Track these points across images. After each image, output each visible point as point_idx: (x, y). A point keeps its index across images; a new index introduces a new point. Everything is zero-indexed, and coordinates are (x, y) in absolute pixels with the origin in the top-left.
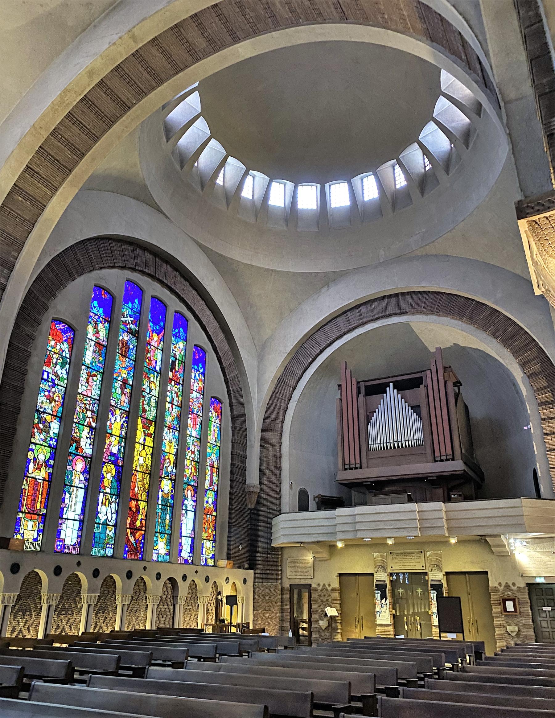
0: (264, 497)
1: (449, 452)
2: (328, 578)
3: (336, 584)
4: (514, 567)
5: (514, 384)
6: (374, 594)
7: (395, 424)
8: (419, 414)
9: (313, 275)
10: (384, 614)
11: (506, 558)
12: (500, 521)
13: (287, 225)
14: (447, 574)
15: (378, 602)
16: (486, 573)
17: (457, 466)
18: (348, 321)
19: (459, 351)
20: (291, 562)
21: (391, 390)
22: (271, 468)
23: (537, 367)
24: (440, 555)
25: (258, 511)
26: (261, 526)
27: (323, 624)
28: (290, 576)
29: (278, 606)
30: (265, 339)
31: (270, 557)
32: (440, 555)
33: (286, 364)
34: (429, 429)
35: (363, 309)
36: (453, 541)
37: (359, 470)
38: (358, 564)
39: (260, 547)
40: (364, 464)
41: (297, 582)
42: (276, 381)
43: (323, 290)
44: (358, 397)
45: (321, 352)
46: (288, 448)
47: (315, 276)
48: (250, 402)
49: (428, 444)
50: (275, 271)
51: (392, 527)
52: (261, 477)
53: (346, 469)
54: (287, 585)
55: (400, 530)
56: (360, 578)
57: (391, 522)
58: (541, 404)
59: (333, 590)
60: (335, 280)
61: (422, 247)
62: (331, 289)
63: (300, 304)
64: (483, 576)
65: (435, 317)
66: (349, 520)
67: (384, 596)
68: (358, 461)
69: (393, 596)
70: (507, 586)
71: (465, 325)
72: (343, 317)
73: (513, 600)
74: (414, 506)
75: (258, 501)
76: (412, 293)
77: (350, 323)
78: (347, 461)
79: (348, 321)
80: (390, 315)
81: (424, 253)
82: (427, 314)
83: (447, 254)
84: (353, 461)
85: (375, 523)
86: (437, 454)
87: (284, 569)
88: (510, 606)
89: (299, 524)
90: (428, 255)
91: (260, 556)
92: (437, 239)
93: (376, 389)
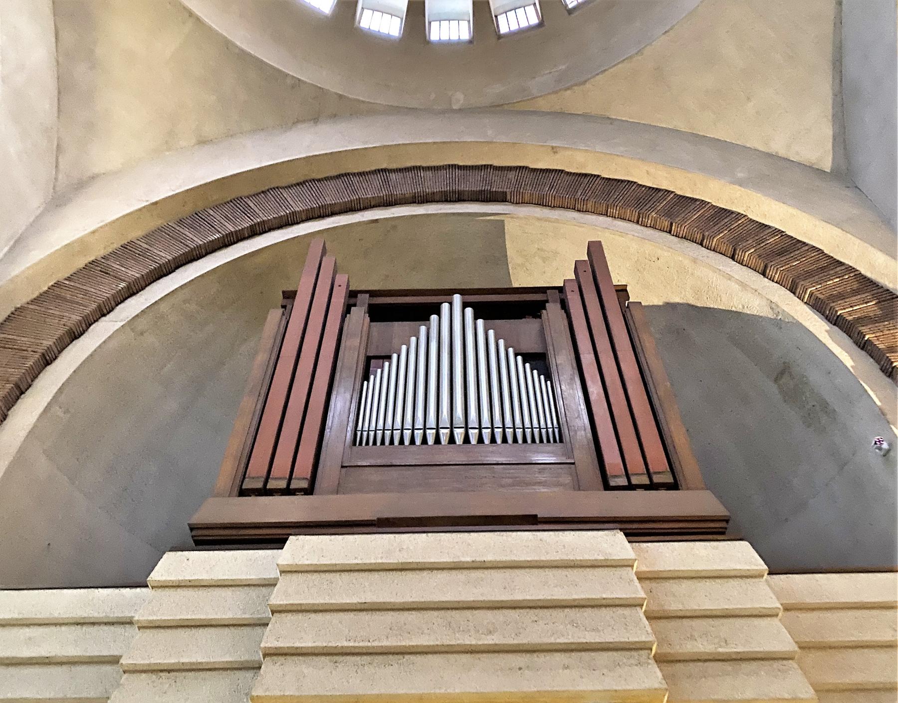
9: (289, 81)
30: (96, 170)
33: (135, 234)
35: (393, 176)
37: (299, 499)
42: (81, 262)
44: (347, 310)
45: (254, 232)
46: (23, 434)
47: (293, 87)
51: (489, 640)
53: (243, 493)
55: (541, 659)
57: (489, 615)
60: (335, 116)
61: (556, 92)
63: (230, 135)
78: (258, 466)
81: (557, 108)
83: (607, 114)
85: (390, 617)
90: (564, 113)
92: (594, 77)
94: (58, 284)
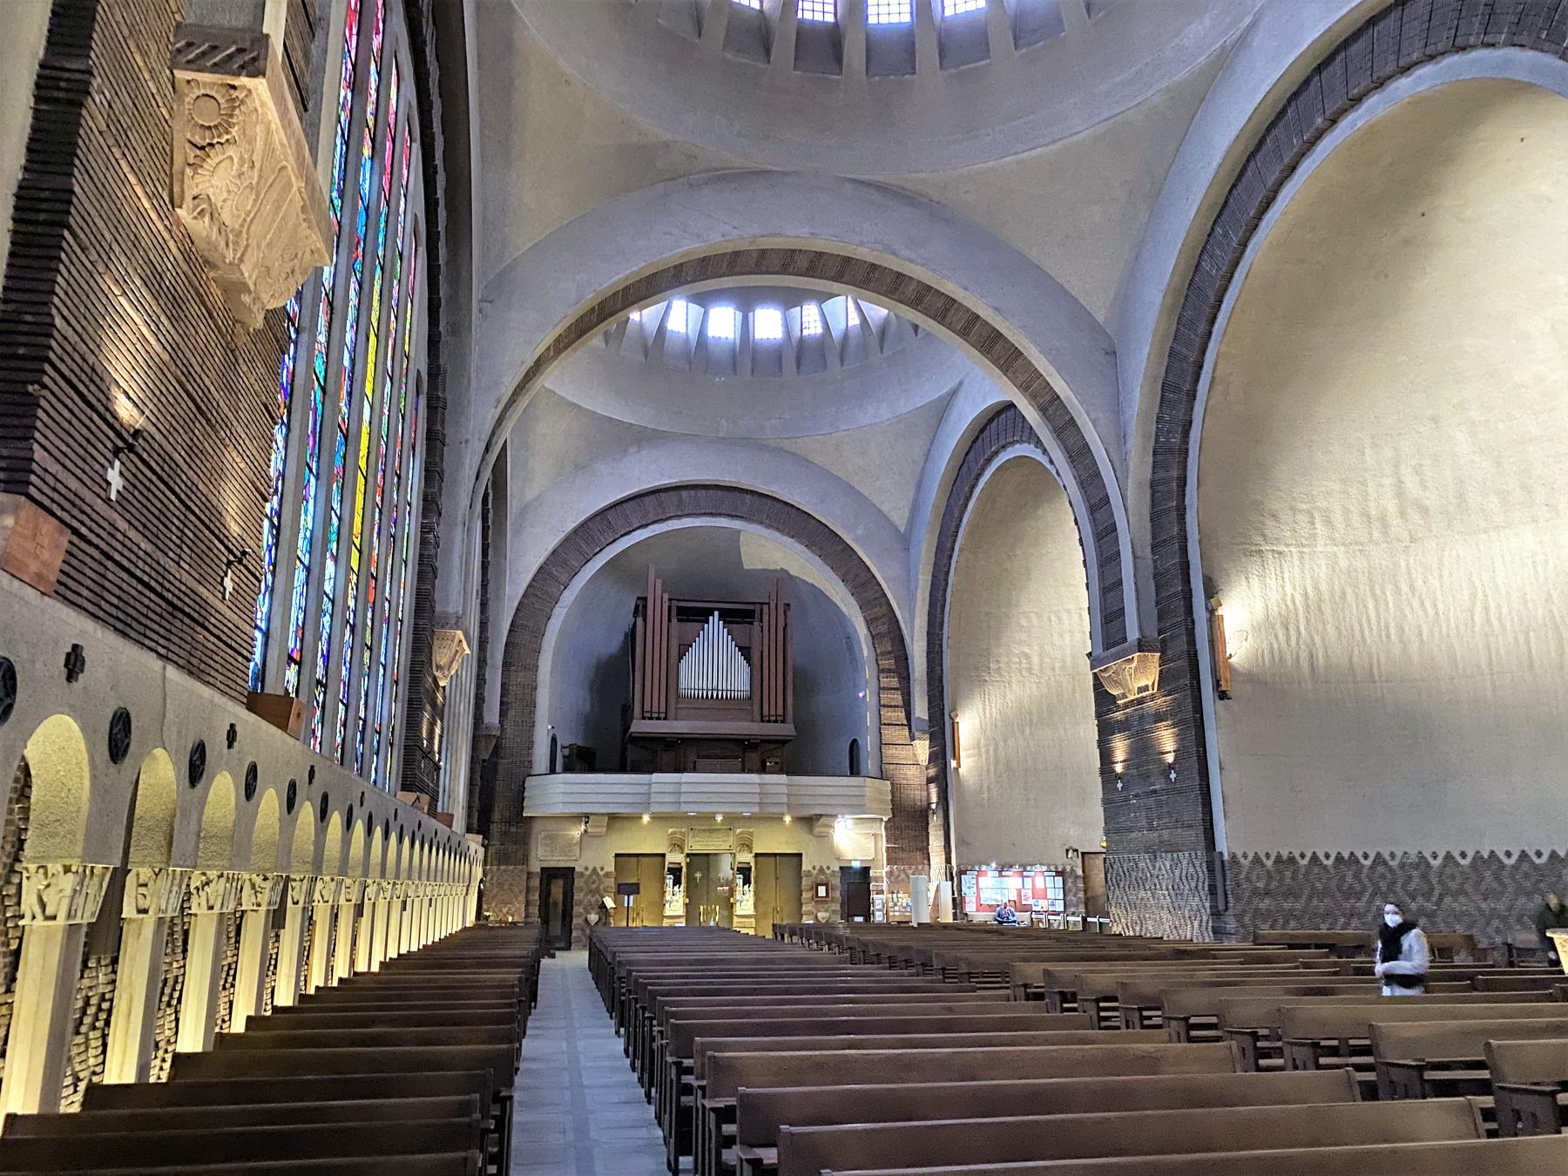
0: (507, 743)
1: (780, 712)
2: (598, 858)
3: (611, 868)
4: (832, 849)
5: (850, 640)
6: (663, 882)
7: (714, 666)
8: (748, 659)
10: (676, 903)
11: (825, 838)
12: (841, 801)
13: (607, 342)
14: (757, 855)
15: (669, 889)
16: (800, 855)
17: (787, 730)
18: (660, 504)
19: (782, 579)
20: (545, 838)
21: (715, 619)
22: (517, 700)
23: (884, 629)
24: (751, 834)
25: (495, 765)
26: (499, 786)
27: (593, 918)
28: (542, 856)
29: (522, 898)
31: (513, 829)
32: (751, 834)
34: (757, 678)
35: (684, 494)
36: (788, 819)
38: (646, 840)
39: (496, 816)
40: (672, 712)
41: (552, 864)
43: (632, 450)
48: (499, 598)
49: (757, 699)
50: (579, 407)
52: (503, 714)
54: (536, 867)
56: (644, 860)
58: (883, 671)
59: (607, 875)
62: (644, 452)
64: (796, 859)
65: (777, 534)
66: (671, 789)
67: (677, 882)
68: (663, 709)
69: (688, 882)
70: (821, 869)
71: (811, 555)
72: (653, 497)
73: (826, 885)
74: (755, 778)
75: (497, 750)
76: (753, 493)
77: (664, 512)
78: (647, 707)
79: (660, 504)
80: (720, 515)
82: (767, 527)
84: (655, 709)
86: (766, 712)
87: (533, 845)
88: (822, 891)
89: (589, 788)
91: (495, 828)
93: (694, 615)
94: (530, 586)
